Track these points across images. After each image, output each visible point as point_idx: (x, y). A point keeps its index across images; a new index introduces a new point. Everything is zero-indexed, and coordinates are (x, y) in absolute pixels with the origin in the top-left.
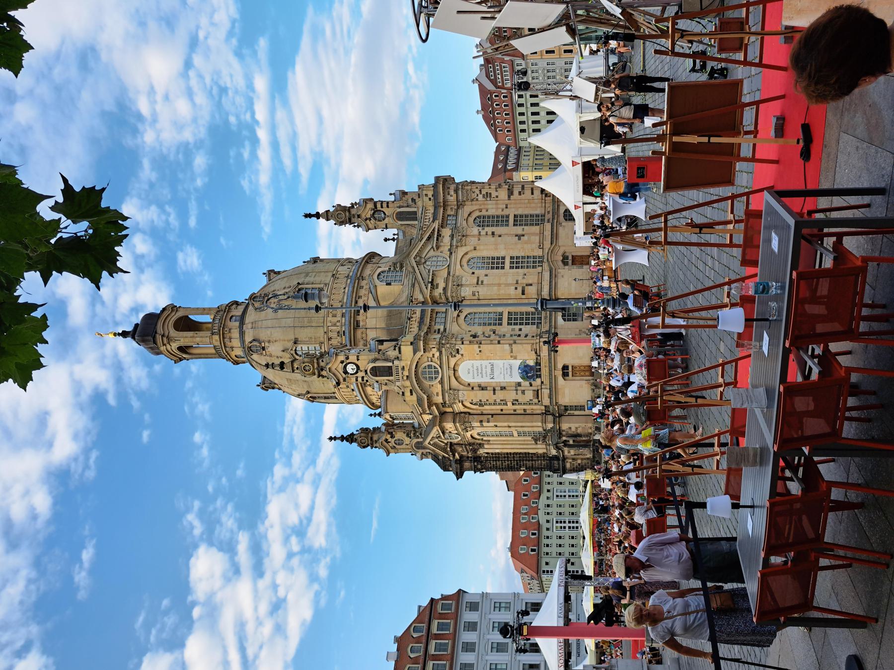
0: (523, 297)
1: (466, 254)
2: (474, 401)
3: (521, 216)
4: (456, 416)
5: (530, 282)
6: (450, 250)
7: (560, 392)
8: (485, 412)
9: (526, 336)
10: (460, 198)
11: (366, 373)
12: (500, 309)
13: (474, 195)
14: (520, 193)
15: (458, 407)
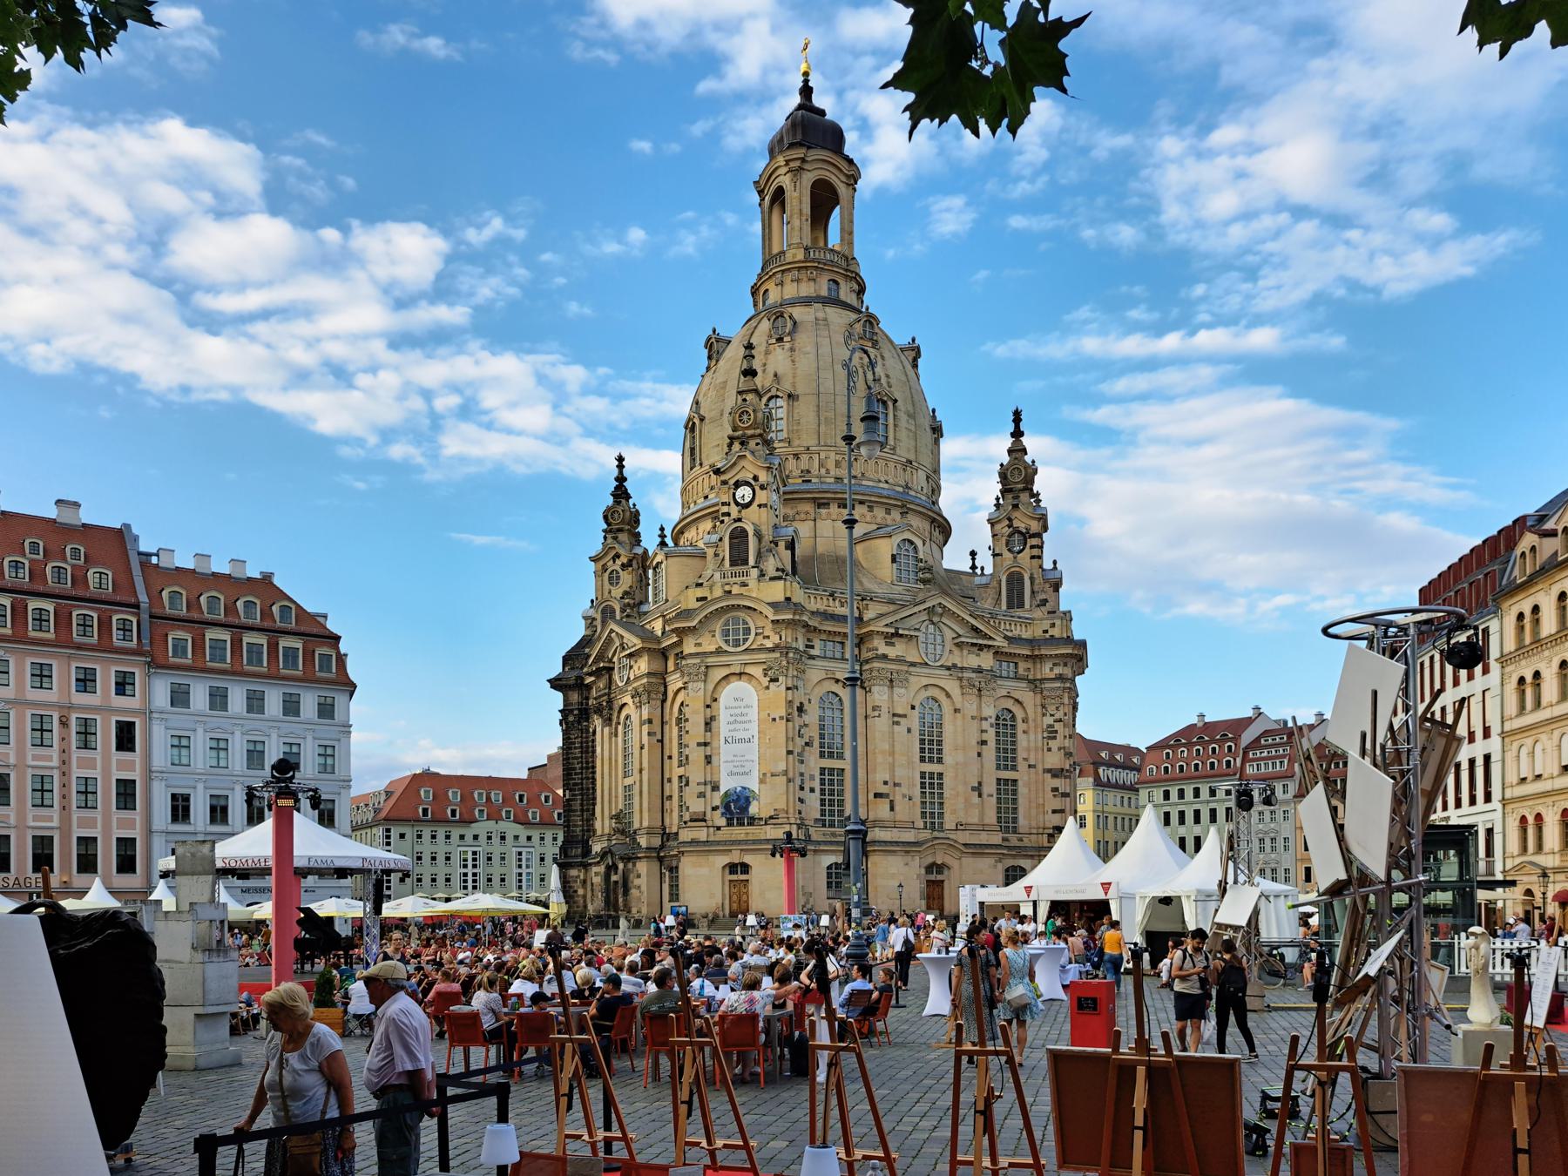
0: (871, 796)
1: (948, 695)
2: (685, 710)
3: (1015, 792)
4: (660, 677)
5: (897, 808)
6: (955, 666)
7: (702, 859)
8: (667, 728)
9: (801, 801)
11: (736, 521)
12: (848, 754)
13: (1051, 709)
14: (1055, 790)
15: (675, 682)
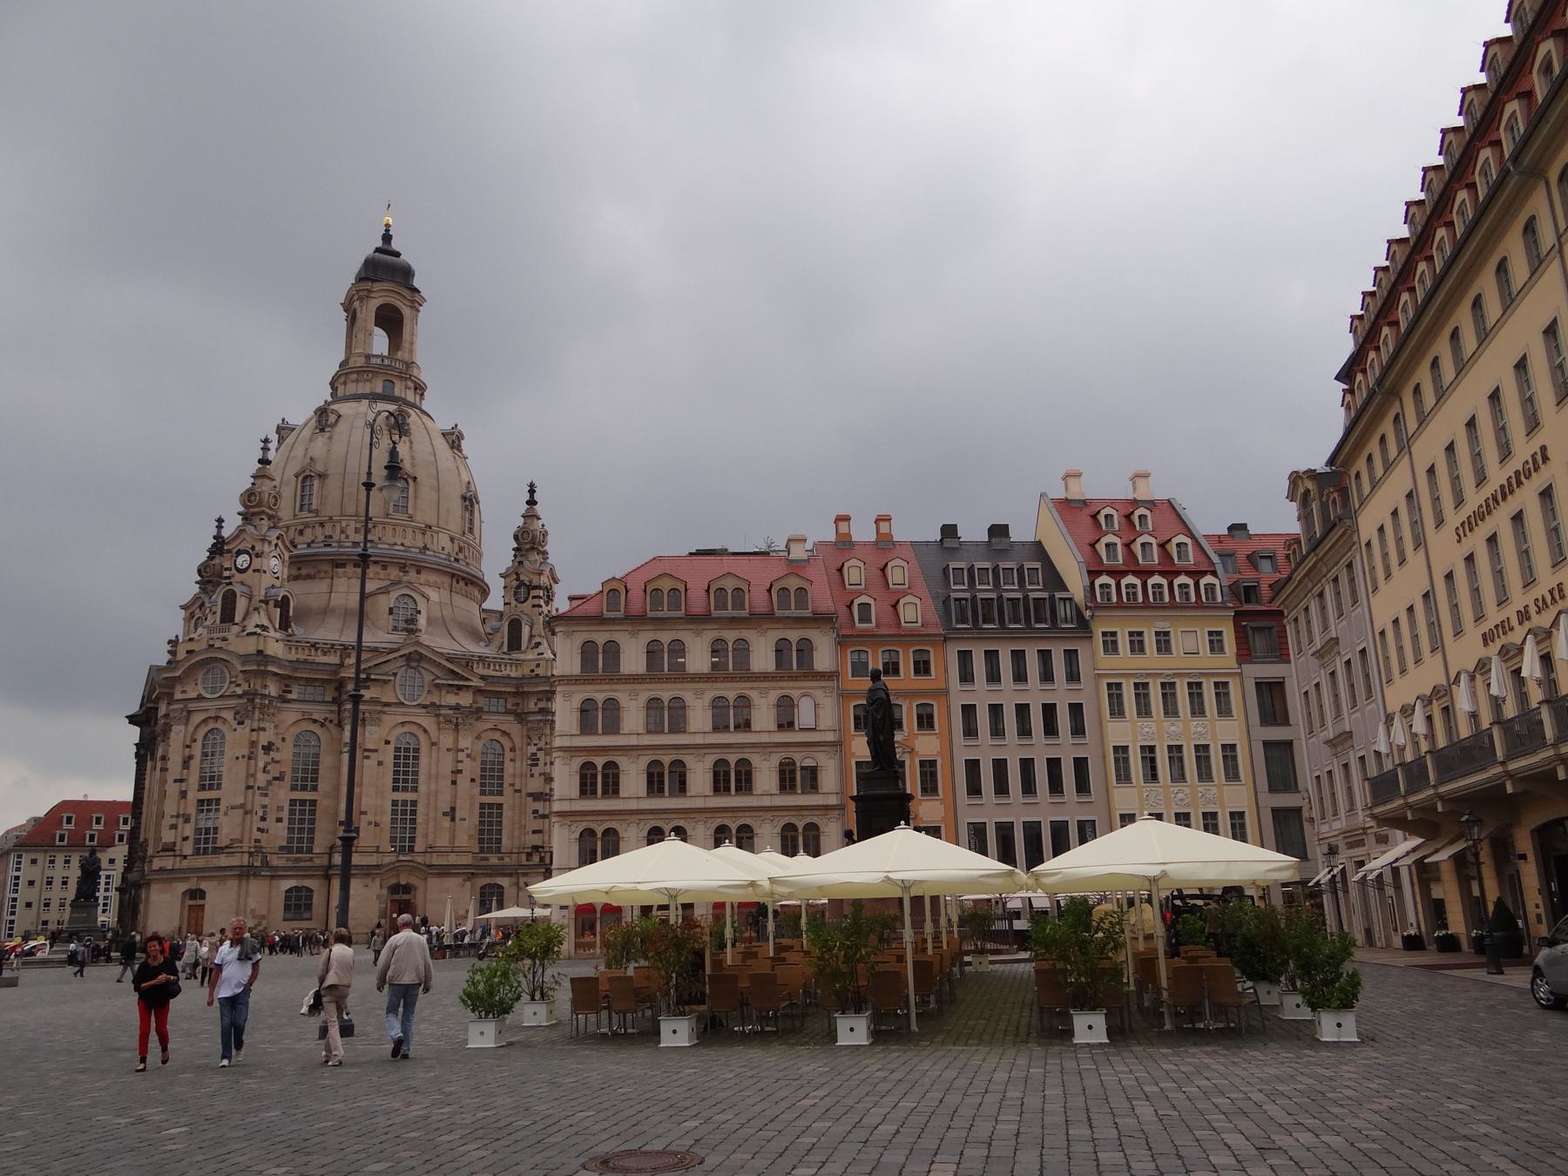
1: (425, 731)
6: (433, 704)
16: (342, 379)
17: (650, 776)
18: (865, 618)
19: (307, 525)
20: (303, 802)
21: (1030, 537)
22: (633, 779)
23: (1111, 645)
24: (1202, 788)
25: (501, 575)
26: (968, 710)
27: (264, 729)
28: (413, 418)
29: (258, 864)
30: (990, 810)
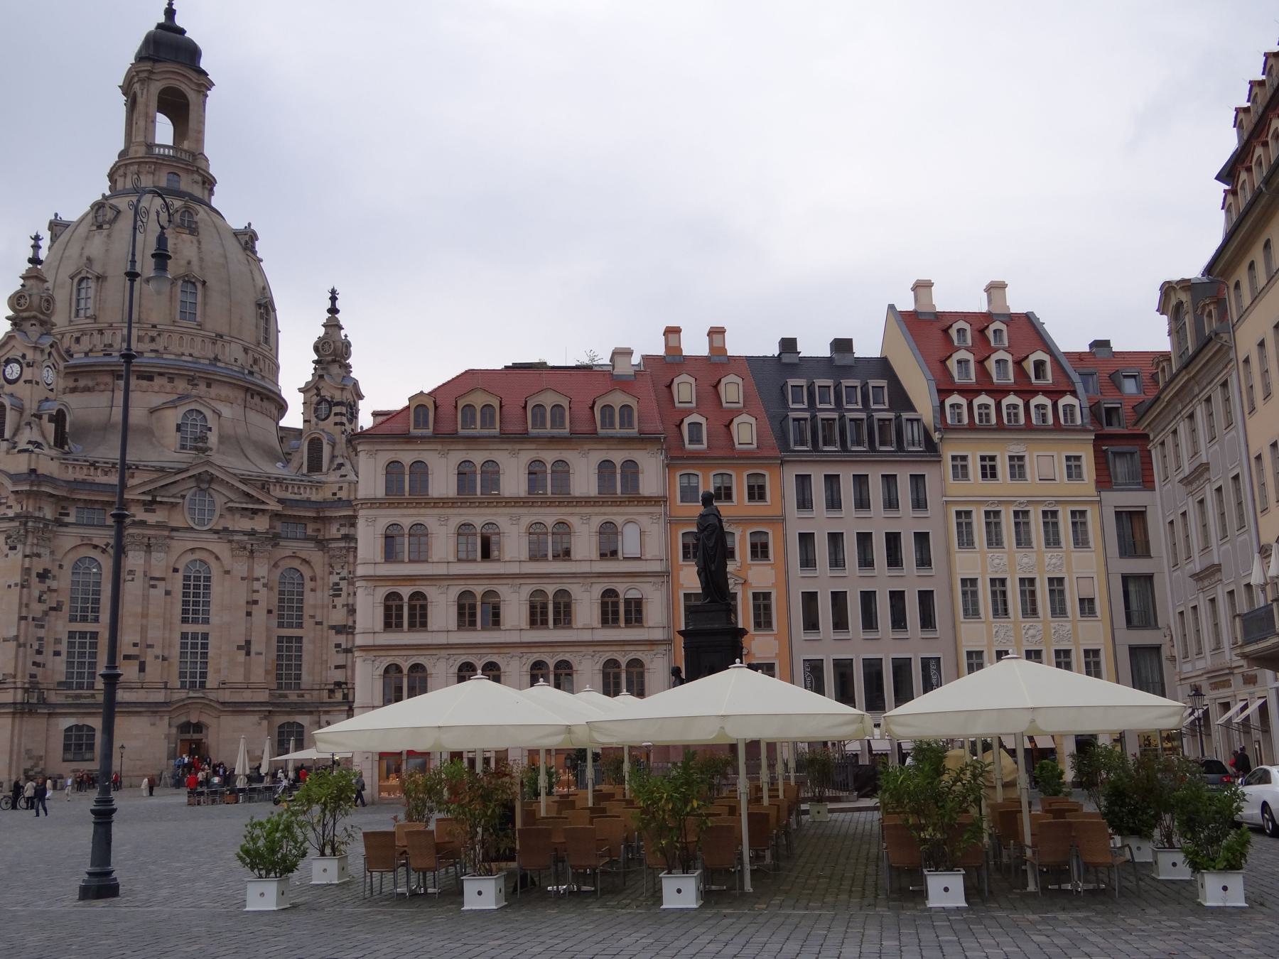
1: (217, 558)
3: (300, 649)
6: (225, 529)
10: (333, 545)
13: (337, 569)
14: (338, 646)
16: (121, 172)
17: (461, 608)
18: (695, 439)
19: (84, 332)
20: (83, 634)
21: (875, 352)
22: (442, 610)
23: (960, 467)
24: (1055, 623)
25: (300, 390)
26: (806, 539)
27: (39, 555)
28: (202, 212)
29: (34, 701)
30: (828, 647)
